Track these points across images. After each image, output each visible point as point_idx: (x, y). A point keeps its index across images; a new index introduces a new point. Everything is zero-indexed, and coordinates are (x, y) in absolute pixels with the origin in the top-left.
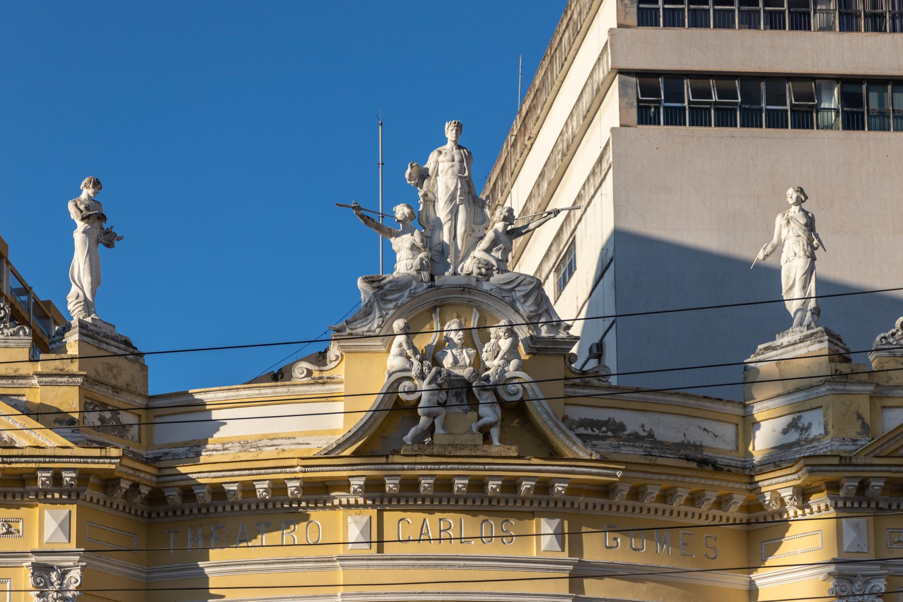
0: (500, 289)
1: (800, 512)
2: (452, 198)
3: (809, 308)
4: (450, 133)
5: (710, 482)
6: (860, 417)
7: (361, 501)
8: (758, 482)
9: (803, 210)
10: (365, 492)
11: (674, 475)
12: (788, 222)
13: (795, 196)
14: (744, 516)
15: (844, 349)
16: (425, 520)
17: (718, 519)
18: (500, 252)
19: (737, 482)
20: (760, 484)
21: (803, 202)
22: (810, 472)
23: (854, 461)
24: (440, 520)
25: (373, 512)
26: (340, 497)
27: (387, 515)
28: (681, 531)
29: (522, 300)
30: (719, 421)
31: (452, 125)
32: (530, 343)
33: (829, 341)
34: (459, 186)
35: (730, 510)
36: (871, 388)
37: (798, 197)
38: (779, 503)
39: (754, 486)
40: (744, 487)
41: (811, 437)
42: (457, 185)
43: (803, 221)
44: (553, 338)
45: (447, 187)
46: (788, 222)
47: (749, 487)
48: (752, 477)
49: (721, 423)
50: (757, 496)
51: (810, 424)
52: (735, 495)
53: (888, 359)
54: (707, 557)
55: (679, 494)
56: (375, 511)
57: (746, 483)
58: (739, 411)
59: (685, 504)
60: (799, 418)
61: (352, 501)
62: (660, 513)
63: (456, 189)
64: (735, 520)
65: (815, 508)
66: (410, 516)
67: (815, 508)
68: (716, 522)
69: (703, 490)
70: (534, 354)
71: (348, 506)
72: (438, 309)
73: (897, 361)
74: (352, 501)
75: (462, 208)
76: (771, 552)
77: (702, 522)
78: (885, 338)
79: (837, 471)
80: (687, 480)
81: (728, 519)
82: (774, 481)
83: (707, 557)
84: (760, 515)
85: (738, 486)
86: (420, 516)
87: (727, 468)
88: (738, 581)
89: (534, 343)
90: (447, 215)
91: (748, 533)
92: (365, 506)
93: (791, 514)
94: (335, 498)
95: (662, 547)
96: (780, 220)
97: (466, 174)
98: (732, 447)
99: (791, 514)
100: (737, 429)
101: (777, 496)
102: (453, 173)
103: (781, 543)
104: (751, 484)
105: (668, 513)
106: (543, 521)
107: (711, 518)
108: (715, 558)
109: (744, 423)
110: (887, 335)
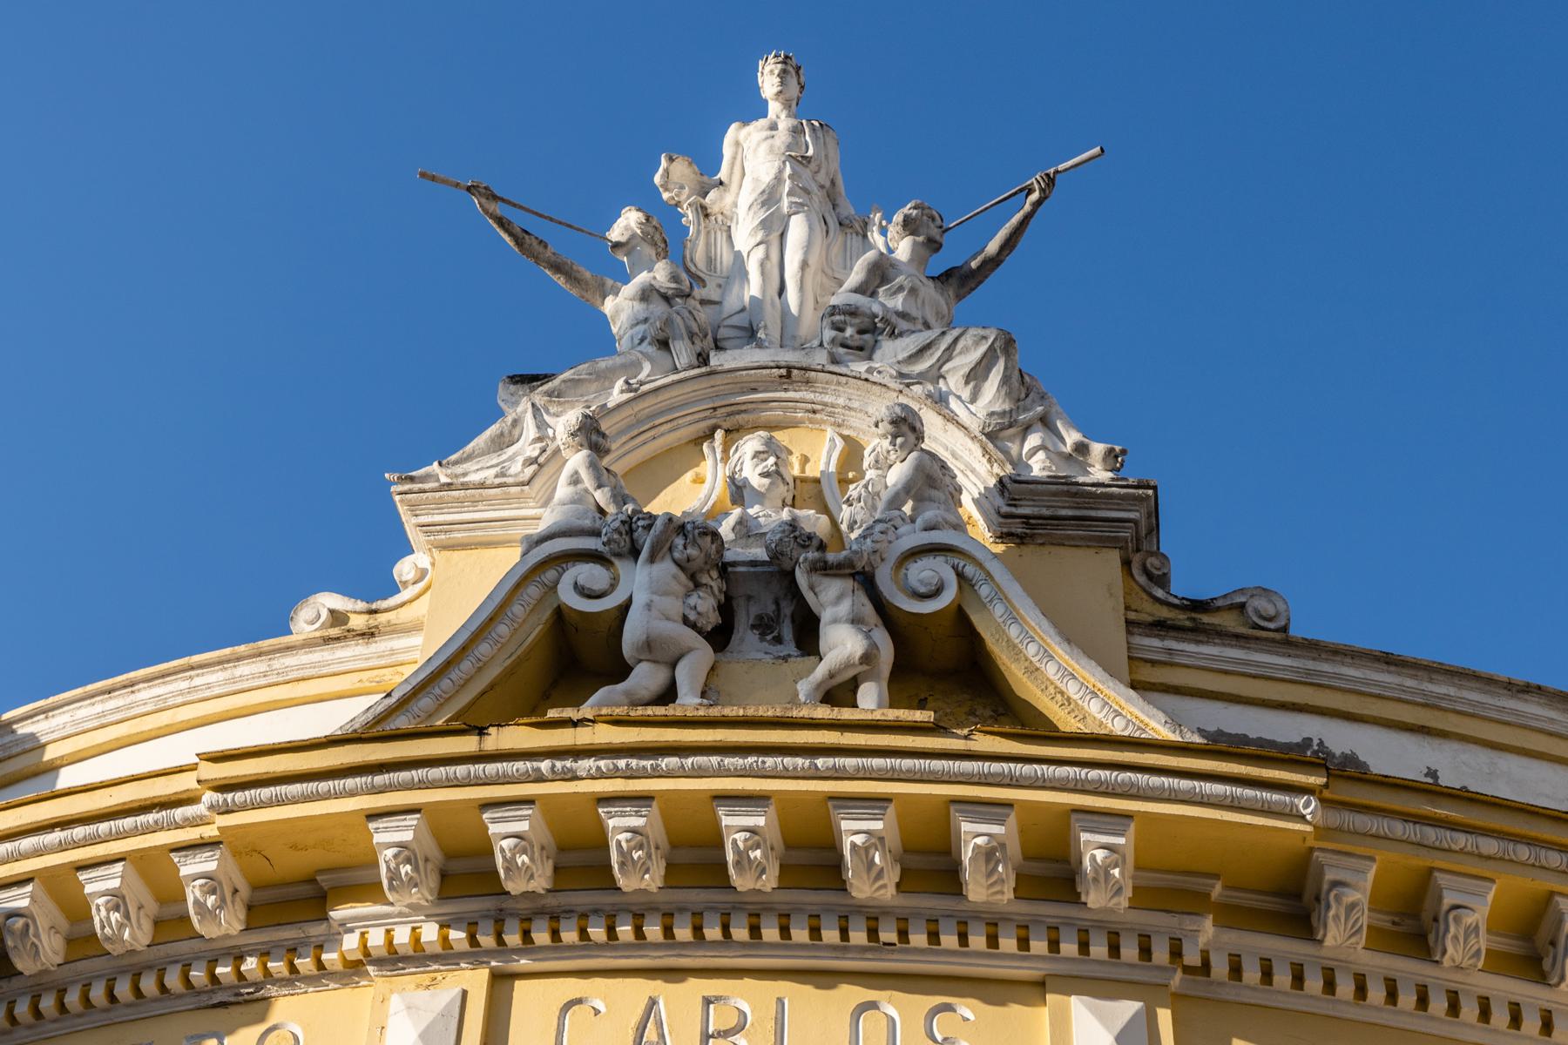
0: (901, 375)
2: (769, 198)
4: (769, 81)
7: (430, 933)
10: (443, 895)
16: (653, 1003)
18: (900, 297)
24: (708, 1002)
25: (476, 980)
26: (359, 926)
27: (523, 990)
29: (966, 394)
31: (771, 60)
32: (999, 502)
34: (788, 171)
42: (781, 171)
44: (1067, 482)
45: (756, 180)
56: (483, 974)
61: (402, 936)
63: (778, 179)
66: (598, 991)
70: (1021, 540)
71: (393, 960)
72: (719, 434)
74: (402, 936)
75: (798, 229)
86: (639, 990)
89: (1013, 502)
90: (755, 230)
92: (447, 956)
94: (345, 927)
97: (811, 152)
102: (771, 150)
106: (1079, 1008)
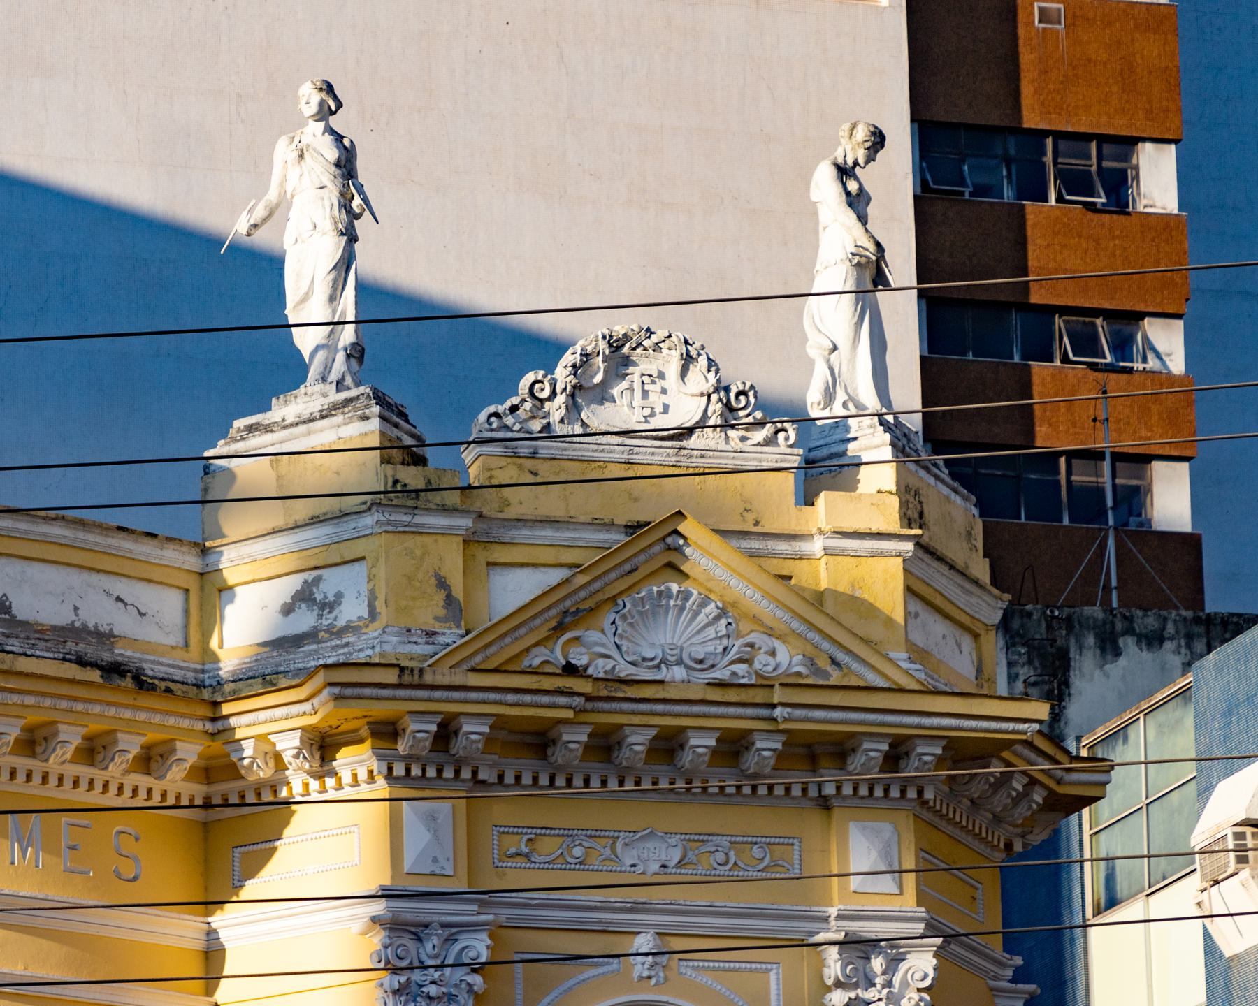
3: (341, 345)
5: (127, 714)
6: (442, 584)
8: (227, 717)
9: (333, 132)
11: (52, 696)
12: (301, 156)
13: (316, 97)
14: (198, 791)
15: (413, 436)
17: (143, 794)
19: (183, 716)
20: (233, 721)
21: (333, 113)
22: (337, 698)
23: (428, 678)
28: (65, 818)
30: (149, 581)
33: (382, 417)
35: (169, 776)
36: (466, 522)
37: (322, 103)
38: (272, 763)
39: (219, 725)
40: (199, 726)
41: (341, 623)
43: (332, 154)
46: (301, 156)
47: (209, 727)
48: (216, 705)
49: (152, 586)
50: (228, 748)
51: (339, 596)
52: (179, 745)
53: (503, 462)
54: (119, 876)
55: (62, 737)
57: (203, 719)
58: (191, 561)
59: (73, 761)
60: (317, 580)
62: (21, 777)
64: (178, 797)
65: (346, 778)
67: (346, 778)
68: (140, 801)
69: (114, 731)
73: (520, 467)
76: (252, 873)
77: (110, 800)
78: (496, 415)
79: (394, 699)
80: (80, 707)
81: (164, 795)
82: (262, 715)
83: (119, 876)
84: (230, 788)
85: (186, 723)
87: (163, 685)
88: (182, 930)
91: (206, 827)
95: (24, 853)
96: (283, 151)
98: (175, 639)
99: (297, 788)
100: (187, 600)
101: (268, 748)
103: (275, 849)
105: (37, 779)
107: (128, 792)
108: (135, 879)
109: (202, 588)
110: (500, 409)
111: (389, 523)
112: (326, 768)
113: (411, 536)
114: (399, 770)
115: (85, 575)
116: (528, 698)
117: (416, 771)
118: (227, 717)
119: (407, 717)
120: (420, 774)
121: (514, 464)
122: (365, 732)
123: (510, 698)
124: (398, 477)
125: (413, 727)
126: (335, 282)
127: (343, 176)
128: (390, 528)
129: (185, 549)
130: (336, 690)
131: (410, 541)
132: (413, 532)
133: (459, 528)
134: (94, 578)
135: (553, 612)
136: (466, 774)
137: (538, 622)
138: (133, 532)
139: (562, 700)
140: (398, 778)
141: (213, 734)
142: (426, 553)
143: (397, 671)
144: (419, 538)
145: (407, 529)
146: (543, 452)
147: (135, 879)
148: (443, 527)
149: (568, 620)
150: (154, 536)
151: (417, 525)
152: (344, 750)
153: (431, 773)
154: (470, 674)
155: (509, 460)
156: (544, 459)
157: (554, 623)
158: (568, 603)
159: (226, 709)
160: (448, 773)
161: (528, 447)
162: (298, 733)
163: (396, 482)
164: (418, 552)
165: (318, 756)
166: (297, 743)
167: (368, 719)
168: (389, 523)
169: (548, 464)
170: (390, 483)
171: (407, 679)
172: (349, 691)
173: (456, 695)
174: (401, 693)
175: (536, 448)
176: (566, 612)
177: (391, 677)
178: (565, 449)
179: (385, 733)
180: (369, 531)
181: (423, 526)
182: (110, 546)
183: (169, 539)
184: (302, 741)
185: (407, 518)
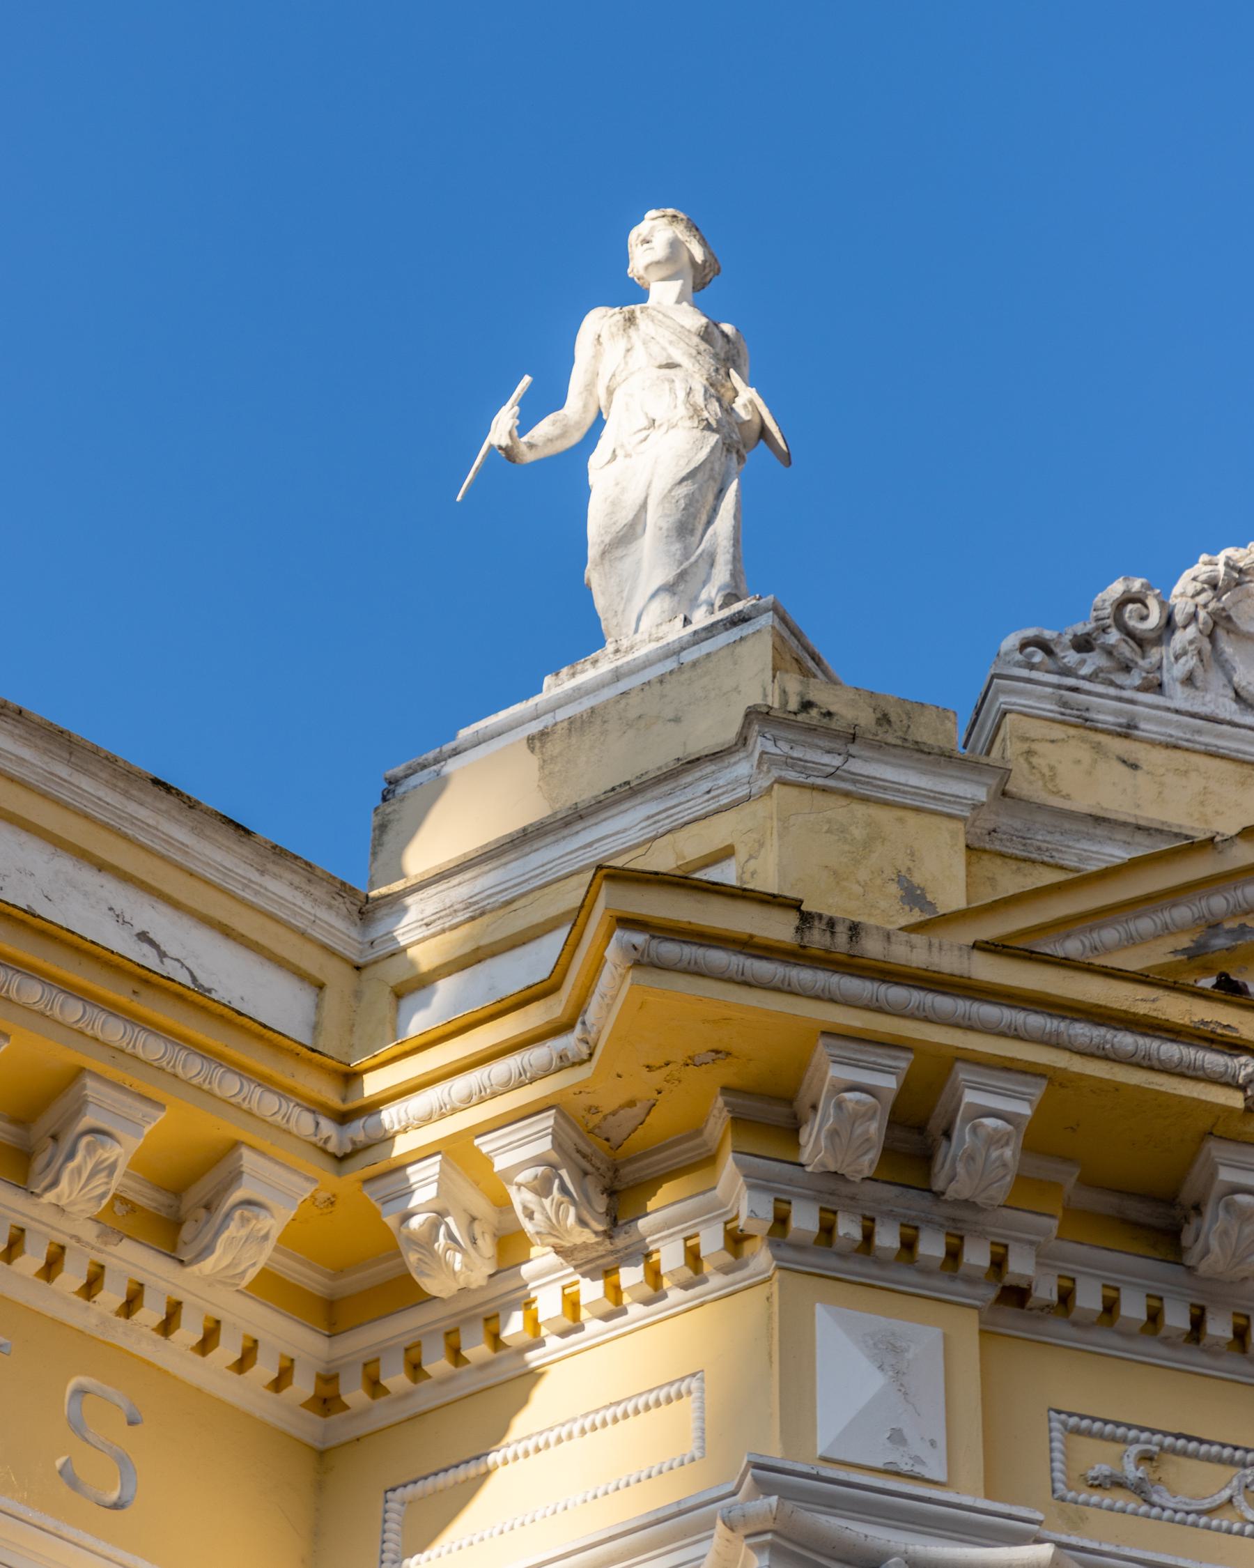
1: (591, 1291)
5: (115, 1031)
8: (373, 1108)
20: (390, 1116)
38: (487, 1246)
39: (358, 1131)
40: (304, 1123)
48: (350, 1078)
50: (371, 1194)
52: (248, 1159)
53: (1058, 732)
57: (317, 1108)
73: (1097, 747)
85: (269, 1105)
93: (549, 1304)
99: (549, 1304)
104: (343, 1118)
111: (790, 762)
112: (621, 1241)
113: (843, 801)
114: (804, 1220)
115: (66, 864)
116: (1126, 1041)
117: (848, 1228)
118: (373, 1108)
119: (823, 1050)
120: (857, 1234)
121: (1084, 740)
122: (718, 1123)
123: (1082, 1032)
124: (813, 696)
125: (838, 1073)
126: (692, 502)
127: (716, 356)
128: (791, 775)
129: (319, 892)
130: (639, 939)
131: (837, 810)
132: (847, 794)
133: (956, 799)
134: (89, 878)
135: (1182, 913)
136: (977, 1256)
137: (1145, 925)
138: (192, 805)
139: (1213, 1060)
140: (799, 1247)
141: (341, 1160)
142: (875, 837)
143: (793, 919)
144: (860, 810)
145: (830, 783)
146: (1148, 728)
147: (117, 1506)
148: (917, 792)
149: (1220, 942)
150: (243, 831)
151: (855, 778)
152: (666, 1192)
153: (887, 1238)
154: (978, 957)
155: (1072, 731)
156: (1153, 743)
157: (1185, 941)
158: (1218, 903)
159: (373, 1085)
160: (932, 1247)
161: (1116, 713)
162: (547, 1121)
163: (806, 705)
164: (858, 833)
165: (601, 1203)
166: (544, 1145)
167: (726, 1073)
168: (790, 762)
169: (1159, 755)
170: (793, 705)
171: (817, 938)
172: (669, 950)
173: (944, 1004)
174: (804, 976)
175: (1133, 716)
176: (1214, 926)
177: (779, 928)
178: (1199, 732)
179: (770, 1113)
180: (742, 792)
181: (869, 780)
182: (133, 819)
183: (279, 852)
184: (557, 1145)
185: (836, 761)
